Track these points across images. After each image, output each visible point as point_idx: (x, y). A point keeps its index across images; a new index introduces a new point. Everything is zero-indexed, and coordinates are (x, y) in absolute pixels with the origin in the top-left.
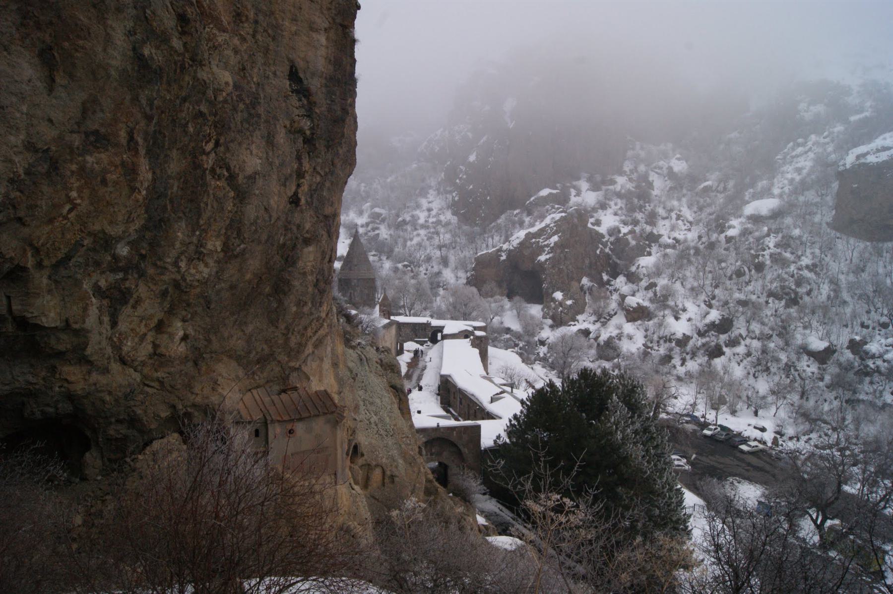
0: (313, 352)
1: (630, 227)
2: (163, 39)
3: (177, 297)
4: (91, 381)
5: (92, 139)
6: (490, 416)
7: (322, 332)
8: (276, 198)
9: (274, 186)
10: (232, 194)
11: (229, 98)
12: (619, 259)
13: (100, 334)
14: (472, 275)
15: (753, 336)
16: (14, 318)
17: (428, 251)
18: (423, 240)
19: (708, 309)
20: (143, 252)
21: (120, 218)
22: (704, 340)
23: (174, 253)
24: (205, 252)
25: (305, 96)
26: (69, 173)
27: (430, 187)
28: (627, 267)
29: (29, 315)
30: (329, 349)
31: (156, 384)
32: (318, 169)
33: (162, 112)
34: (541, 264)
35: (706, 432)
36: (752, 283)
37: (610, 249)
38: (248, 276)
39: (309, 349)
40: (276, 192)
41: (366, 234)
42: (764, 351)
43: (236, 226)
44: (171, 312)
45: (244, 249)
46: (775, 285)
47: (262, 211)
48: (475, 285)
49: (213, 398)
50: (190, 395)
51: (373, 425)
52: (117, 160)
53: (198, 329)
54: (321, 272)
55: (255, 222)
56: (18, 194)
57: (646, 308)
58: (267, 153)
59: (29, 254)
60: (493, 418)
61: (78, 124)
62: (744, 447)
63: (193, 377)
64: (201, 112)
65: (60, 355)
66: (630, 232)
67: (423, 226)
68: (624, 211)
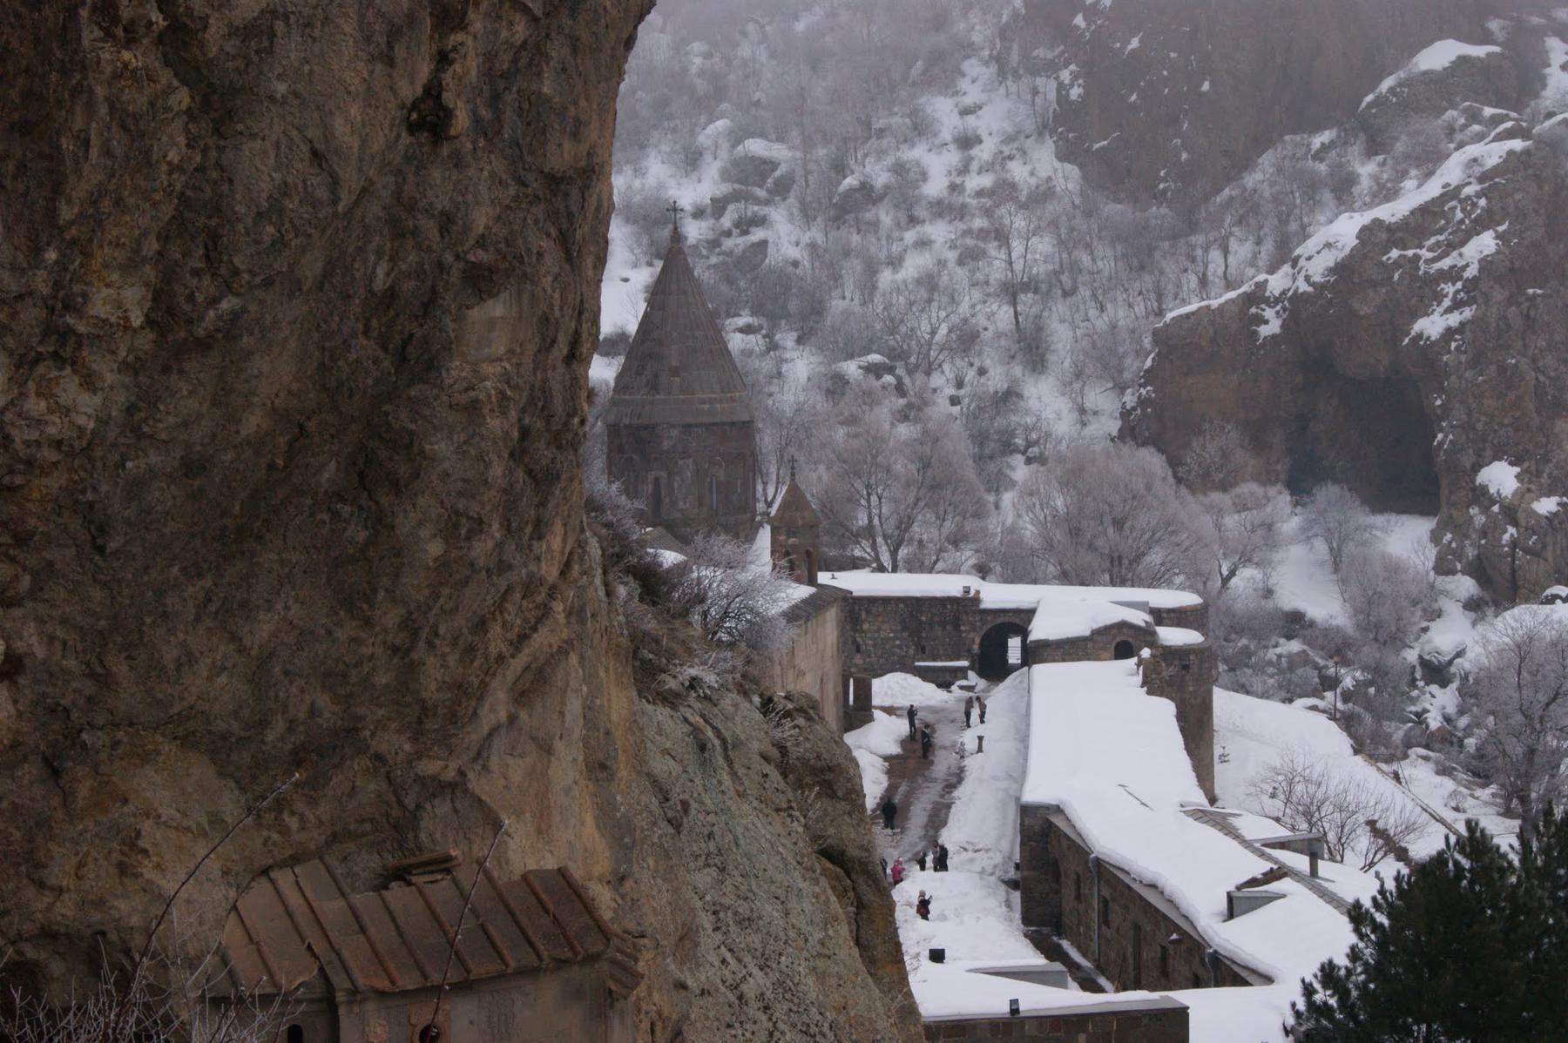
0: (512, 719)
6: (1224, 972)
7: (544, 639)
8: (355, 110)
9: (347, 63)
10: (182, 98)
14: (1143, 402)
17: (964, 309)
18: (941, 263)
24: (82, 328)
27: (968, 50)
30: (574, 706)
34: (1427, 352)
38: (253, 422)
39: (497, 707)
41: (714, 244)
43: (200, 224)
45: (236, 316)
48: (1157, 442)
49: (123, 905)
50: (30, 892)
51: (753, 1010)
53: (60, 633)
54: (539, 399)
55: (273, 211)
60: (1244, 983)
67: (941, 209)
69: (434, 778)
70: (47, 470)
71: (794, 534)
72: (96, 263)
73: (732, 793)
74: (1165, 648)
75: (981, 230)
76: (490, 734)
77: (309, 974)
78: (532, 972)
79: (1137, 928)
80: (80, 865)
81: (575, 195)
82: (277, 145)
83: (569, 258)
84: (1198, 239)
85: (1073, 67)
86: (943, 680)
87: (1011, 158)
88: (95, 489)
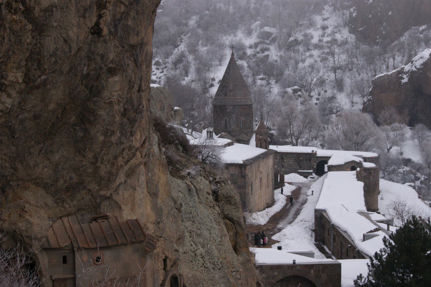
0: (125, 181)
7: (133, 161)
8: (75, 29)
10: (30, 27)
14: (369, 100)
17: (321, 74)
30: (143, 178)
38: (52, 106)
39: (121, 178)
41: (254, 56)
43: (36, 57)
45: (45, 80)
49: (20, 224)
51: (199, 258)
53: (4, 157)
55: (54, 54)
60: (365, 258)
67: (316, 46)
69: (104, 195)
71: (261, 135)
72: (9, 67)
73: (198, 202)
74: (365, 168)
75: (327, 52)
76: (119, 185)
78: (126, 244)
79: (341, 243)
80: (10, 214)
81: (138, 50)
82: (55, 38)
83: (137, 66)
84: (387, 55)
85: (354, 7)
86: (306, 175)
87: (336, 32)
88: (11, 122)
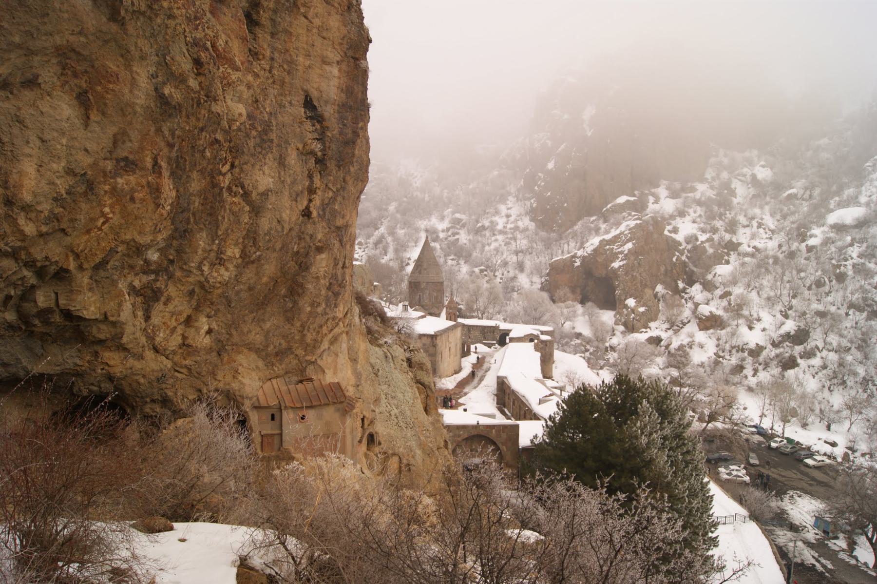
1: (708, 235)
2: (181, 80)
3: (202, 297)
4: (128, 365)
5: (122, 164)
7: (336, 331)
8: (288, 212)
9: (286, 201)
10: (247, 208)
11: (242, 127)
12: (696, 266)
13: (134, 326)
14: (546, 281)
15: (831, 348)
16: (61, 311)
17: (504, 256)
19: (784, 319)
20: (171, 257)
21: (148, 229)
22: (778, 351)
23: (197, 259)
25: (318, 122)
26: (102, 193)
27: (509, 194)
28: (703, 276)
29: (73, 309)
31: (184, 370)
32: (330, 185)
33: (183, 140)
34: (615, 271)
35: (774, 445)
36: (833, 294)
37: (687, 257)
38: (265, 279)
39: (325, 345)
40: (288, 206)
41: (446, 239)
42: (841, 364)
43: (252, 236)
44: (197, 309)
45: (260, 256)
46: (856, 296)
47: (275, 223)
48: (549, 291)
51: (393, 417)
52: (144, 182)
54: (334, 276)
55: (268, 233)
56: (61, 209)
57: (719, 316)
58: (279, 173)
59: (71, 259)
61: (111, 152)
62: (809, 461)
63: (216, 366)
64: (216, 140)
65: (101, 342)
66: (708, 240)
67: (501, 232)
68: (704, 219)
70: (218, 288)
77: (276, 402)
84: (562, 242)
86: (489, 346)
